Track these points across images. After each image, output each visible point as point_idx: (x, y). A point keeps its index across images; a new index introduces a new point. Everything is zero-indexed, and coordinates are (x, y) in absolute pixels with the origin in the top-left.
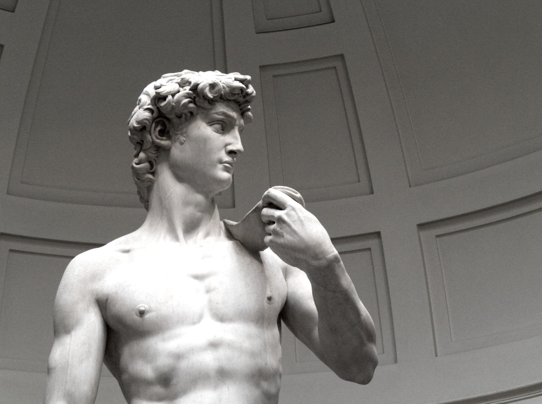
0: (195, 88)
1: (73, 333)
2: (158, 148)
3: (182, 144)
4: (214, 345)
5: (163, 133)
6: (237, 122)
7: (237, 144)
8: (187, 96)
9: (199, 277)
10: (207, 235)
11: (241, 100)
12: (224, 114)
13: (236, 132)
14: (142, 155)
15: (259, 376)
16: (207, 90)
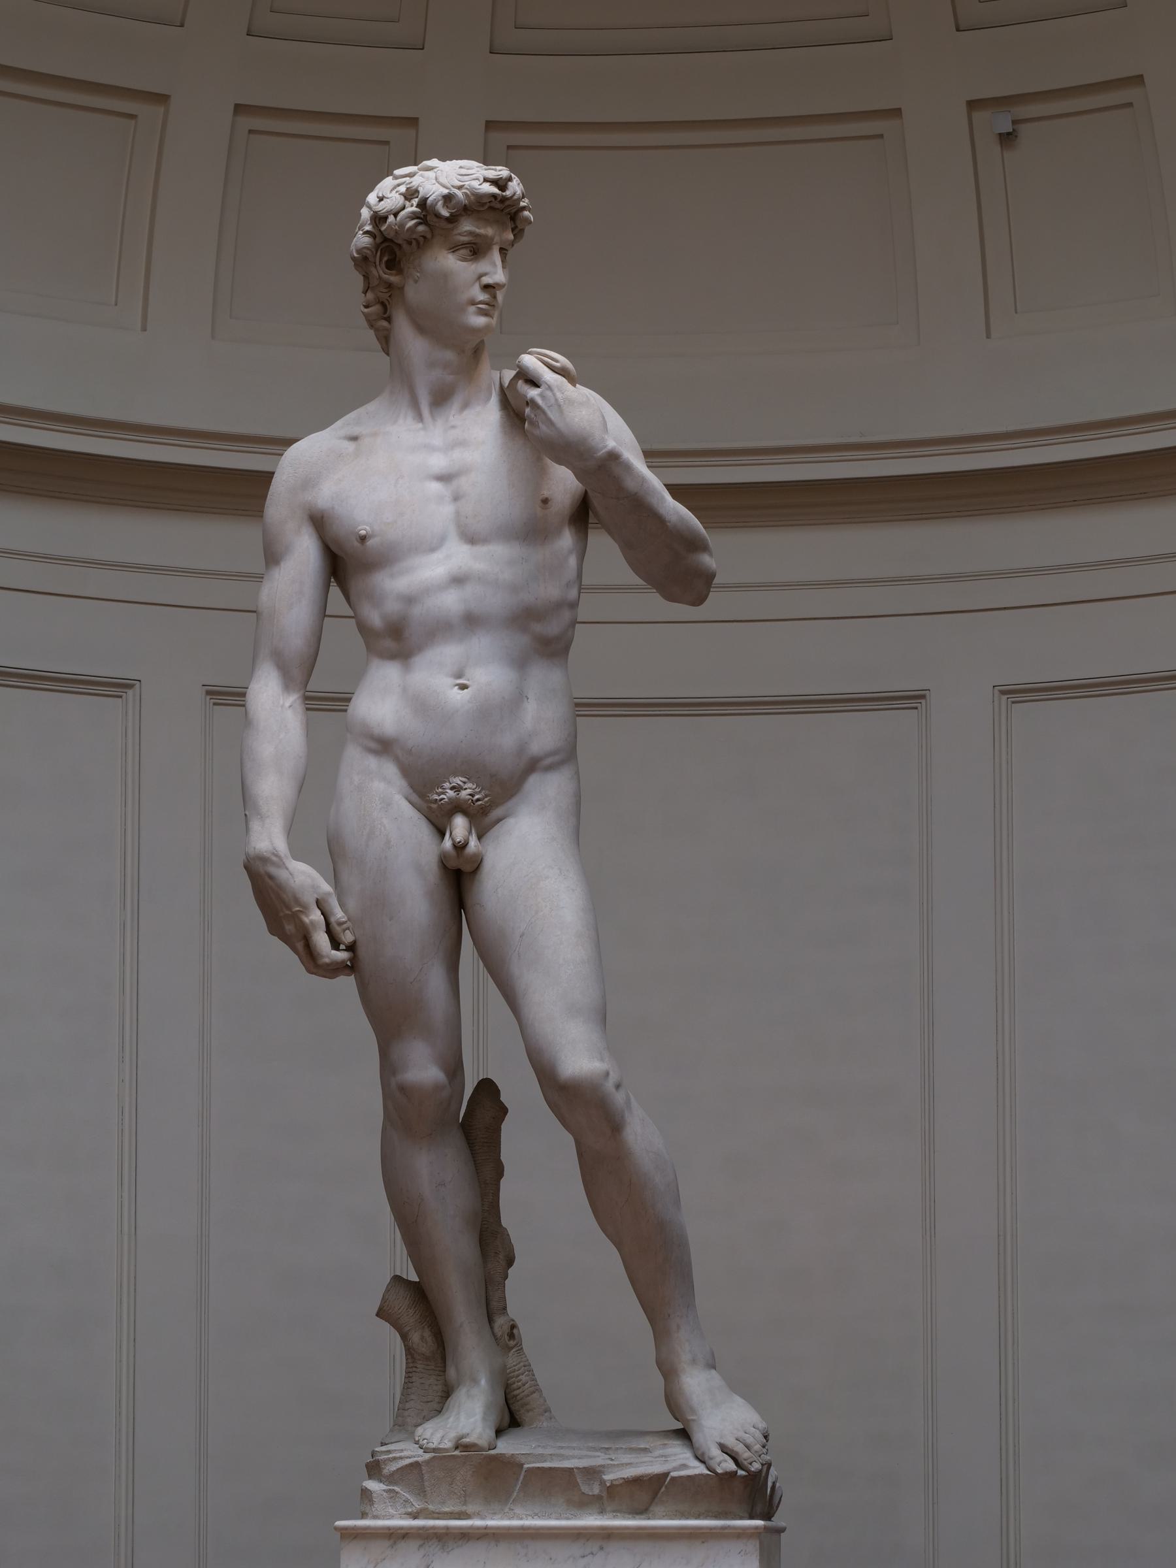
0: (423, 204)
1: (282, 564)
2: (390, 286)
3: (416, 282)
4: (458, 580)
5: (393, 264)
6: (497, 239)
7: (495, 273)
8: (414, 216)
9: (444, 478)
10: (466, 405)
11: (498, 206)
12: (471, 233)
13: (496, 256)
14: (370, 295)
15: (524, 618)
16: (440, 203)
